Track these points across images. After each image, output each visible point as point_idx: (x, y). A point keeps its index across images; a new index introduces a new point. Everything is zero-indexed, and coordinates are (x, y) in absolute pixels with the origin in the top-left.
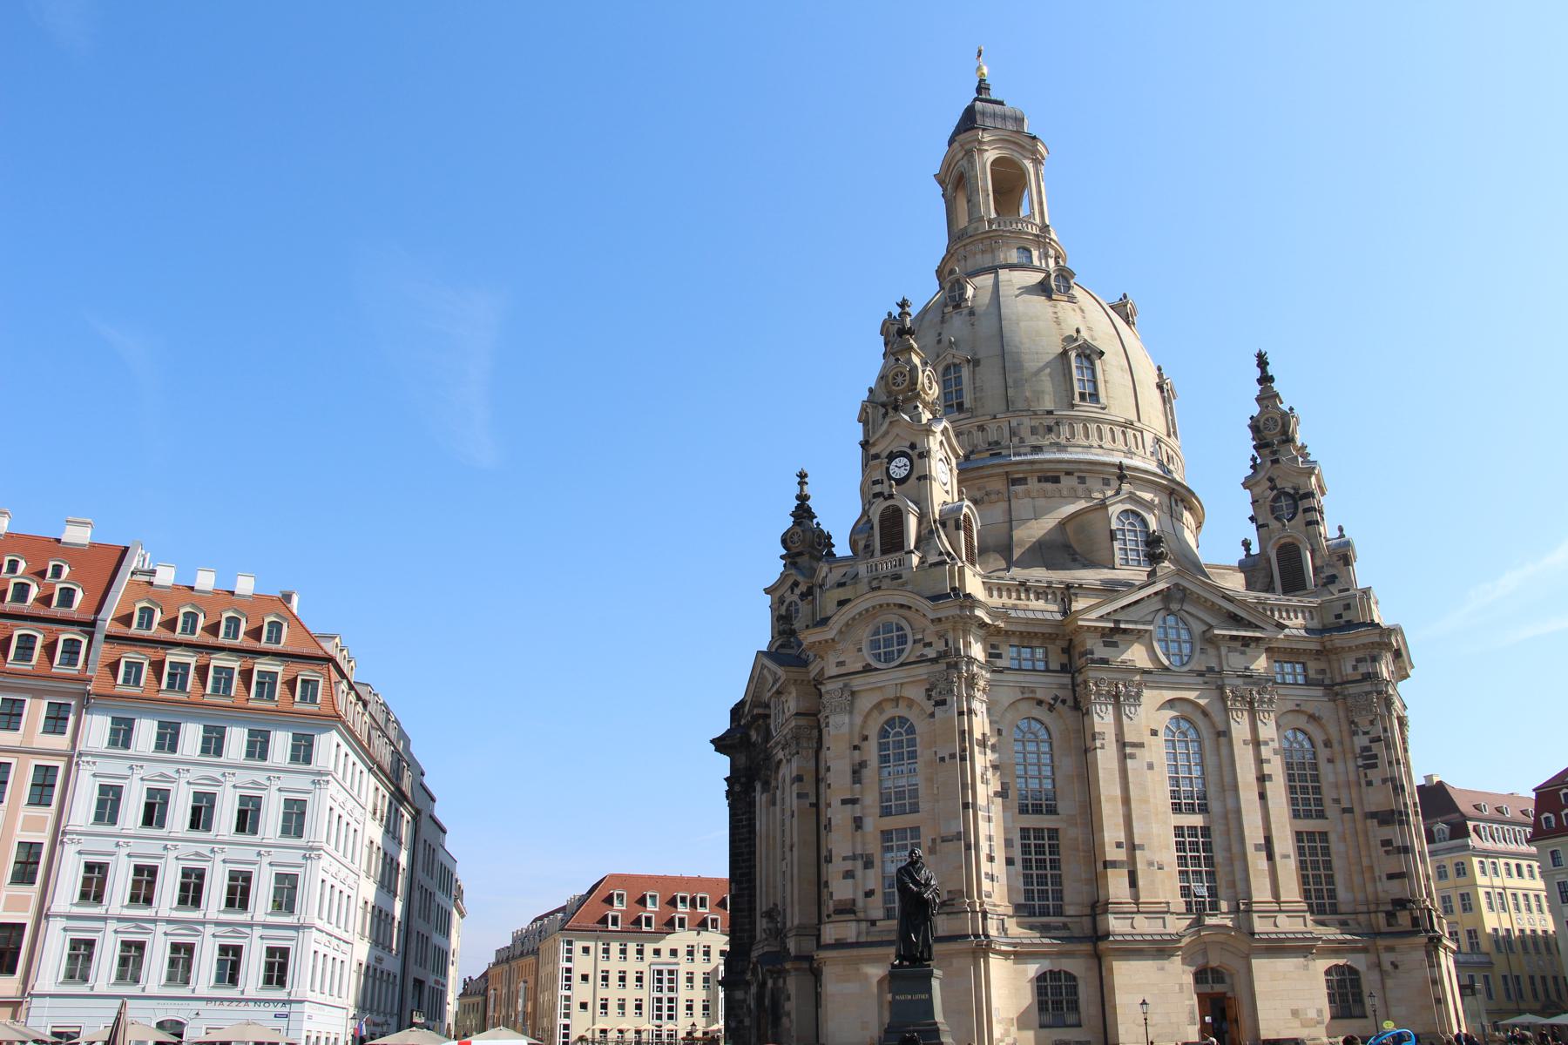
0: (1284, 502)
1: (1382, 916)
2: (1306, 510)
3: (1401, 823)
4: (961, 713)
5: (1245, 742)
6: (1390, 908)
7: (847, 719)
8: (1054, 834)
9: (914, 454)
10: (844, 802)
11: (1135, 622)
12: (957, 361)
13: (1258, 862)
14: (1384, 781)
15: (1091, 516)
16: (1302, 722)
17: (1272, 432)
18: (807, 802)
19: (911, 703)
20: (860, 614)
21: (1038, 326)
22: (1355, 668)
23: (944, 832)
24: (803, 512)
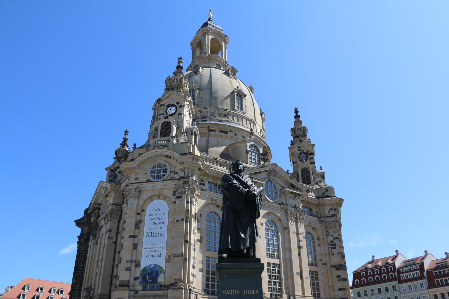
0: (303, 155)
2: (311, 159)
4: (188, 202)
9: (178, 106)
10: (130, 236)
11: (259, 180)
12: (194, 88)
13: (297, 279)
14: (338, 254)
15: (240, 144)
18: (111, 241)
20: (148, 159)
21: (223, 83)
22: (329, 212)
23: (175, 252)
24: (124, 144)
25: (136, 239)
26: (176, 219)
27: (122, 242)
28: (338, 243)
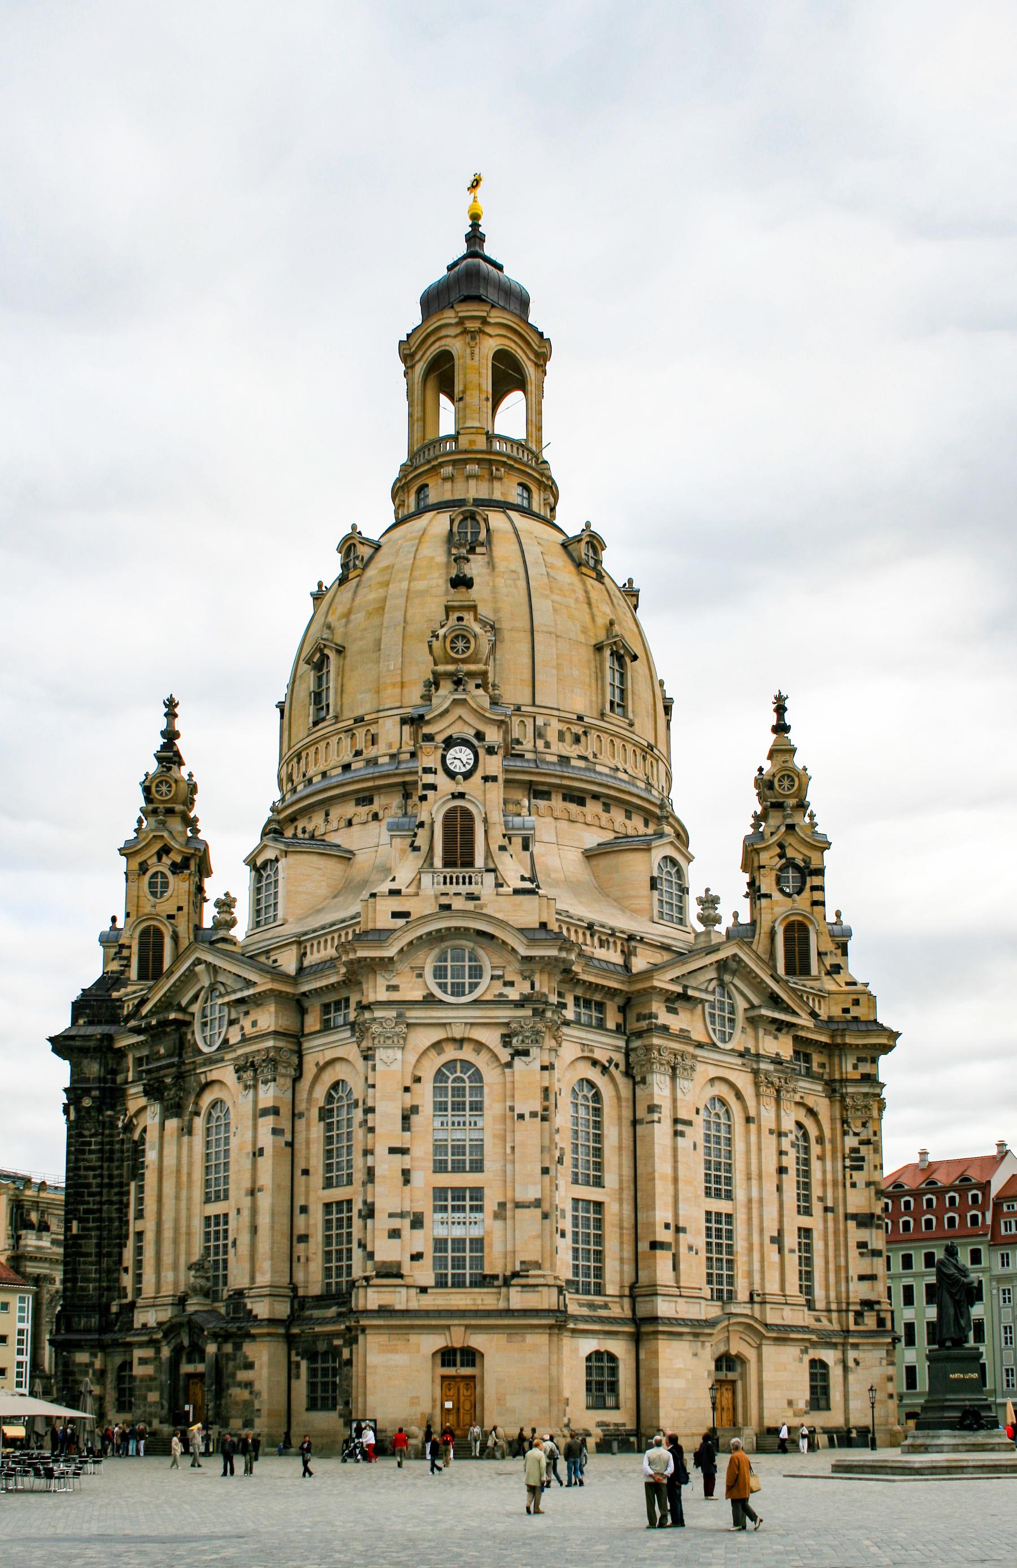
1: (851, 1315)
3: (879, 1227)
4: (544, 1068)
5: (771, 1132)
6: (858, 1308)
7: (399, 1054)
8: (599, 1206)
10: (393, 1151)
14: (868, 1184)
16: (801, 1115)
17: (782, 792)
18: (282, 1140)
19: (479, 1046)
20: (430, 933)
22: (855, 1067)
23: (520, 1197)
25: (406, 1157)
26: (517, 1111)
27: (369, 1164)
28: (872, 1156)
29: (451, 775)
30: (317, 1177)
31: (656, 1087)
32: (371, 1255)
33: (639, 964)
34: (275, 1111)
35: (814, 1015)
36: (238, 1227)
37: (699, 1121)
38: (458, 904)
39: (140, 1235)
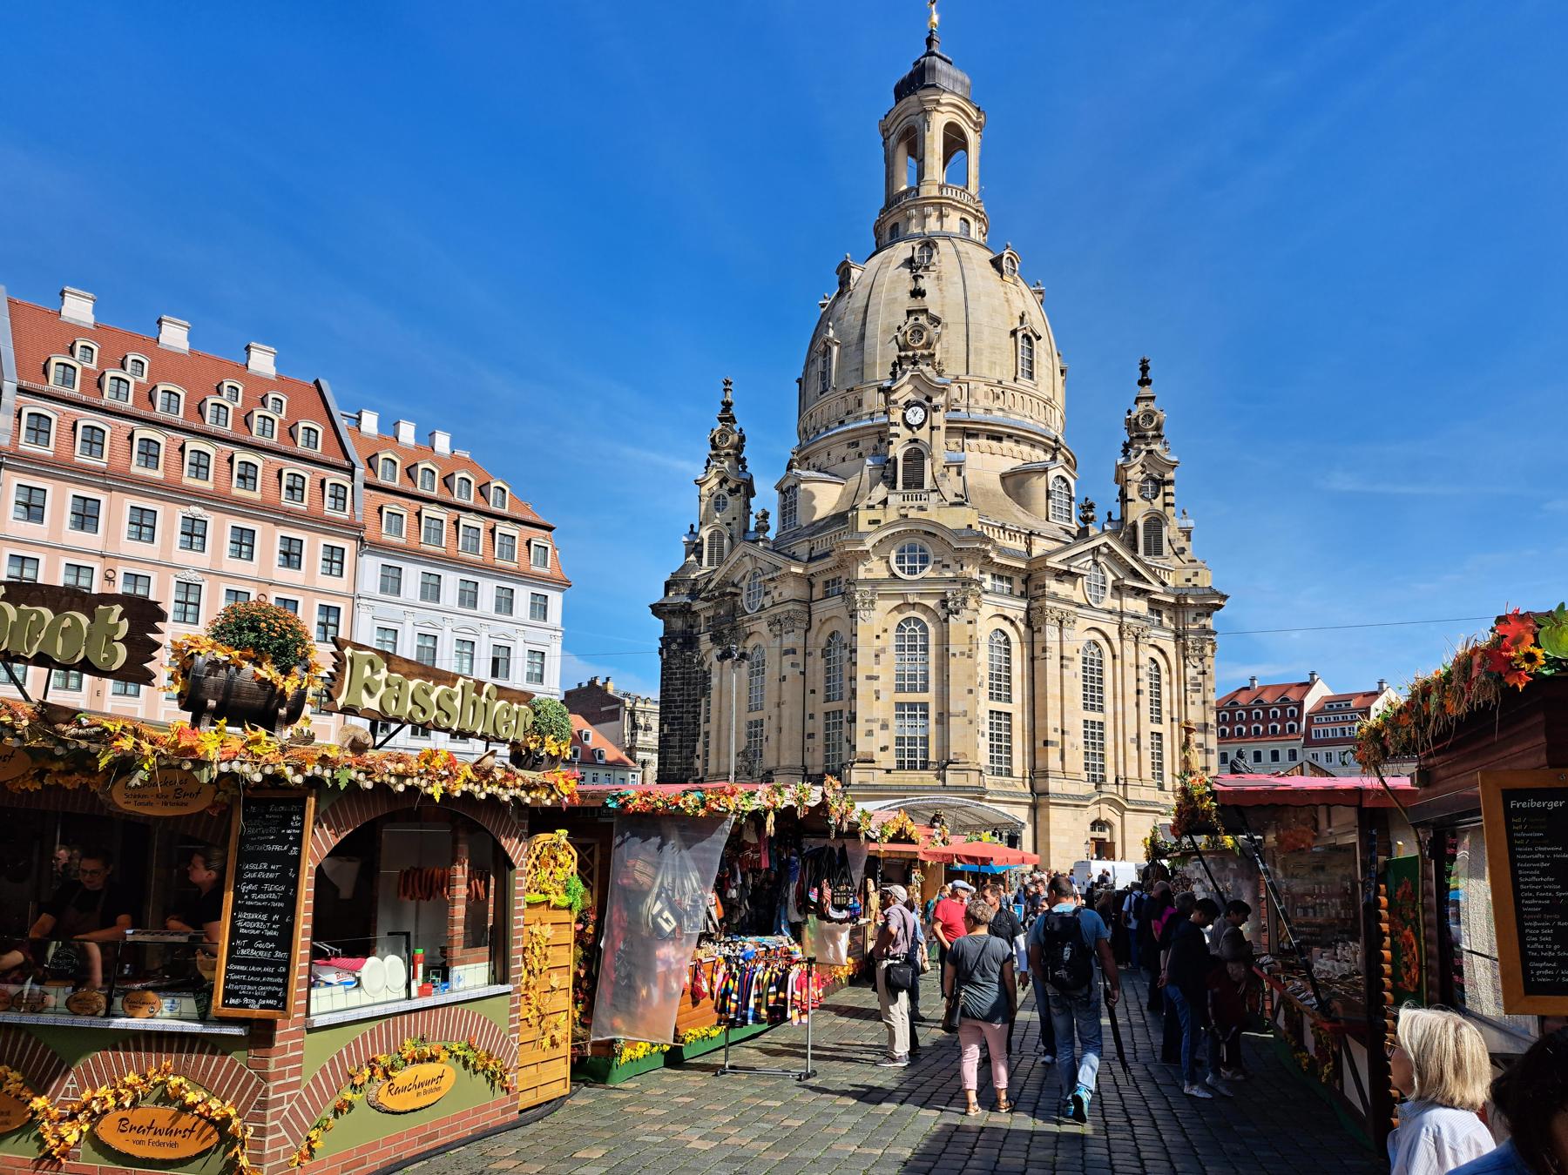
2: (1166, 494)
8: (1009, 714)
10: (869, 678)
16: (1155, 653)
18: (797, 671)
19: (926, 608)
29: (909, 426)
30: (820, 696)
31: (1048, 637)
32: (854, 747)
33: (1036, 552)
34: (794, 652)
35: (1163, 584)
36: (769, 728)
37: (1079, 658)
38: (913, 514)
39: (707, 734)
